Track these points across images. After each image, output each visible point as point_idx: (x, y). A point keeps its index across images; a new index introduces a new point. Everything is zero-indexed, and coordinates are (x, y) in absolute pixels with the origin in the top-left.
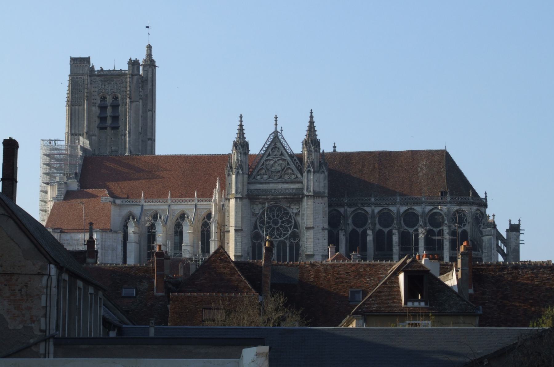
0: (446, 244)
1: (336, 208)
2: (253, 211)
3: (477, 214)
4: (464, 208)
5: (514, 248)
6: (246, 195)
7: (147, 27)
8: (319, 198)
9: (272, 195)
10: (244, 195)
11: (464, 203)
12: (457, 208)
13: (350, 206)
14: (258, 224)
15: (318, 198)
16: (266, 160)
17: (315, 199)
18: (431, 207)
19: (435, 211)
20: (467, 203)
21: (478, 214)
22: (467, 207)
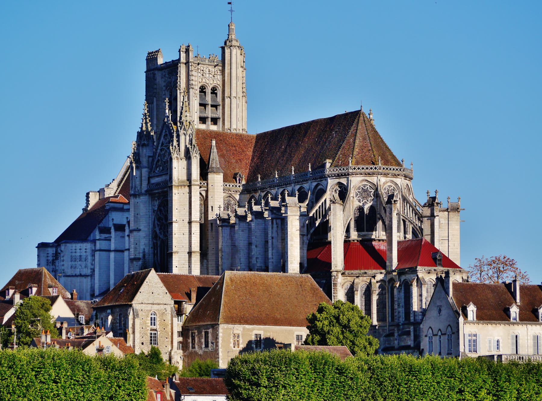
2: (154, 208)
3: (365, 185)
5: (389, 224)
6: (146, 191)
7: (230, 3)
10: (143, 191)
11: (342, 175)
13: (262, 190)
14: (156, 222)
15: (183, 187)
17: (180, 189)
18: (314, 184)
19: (320, 187)
21: (368, 186)
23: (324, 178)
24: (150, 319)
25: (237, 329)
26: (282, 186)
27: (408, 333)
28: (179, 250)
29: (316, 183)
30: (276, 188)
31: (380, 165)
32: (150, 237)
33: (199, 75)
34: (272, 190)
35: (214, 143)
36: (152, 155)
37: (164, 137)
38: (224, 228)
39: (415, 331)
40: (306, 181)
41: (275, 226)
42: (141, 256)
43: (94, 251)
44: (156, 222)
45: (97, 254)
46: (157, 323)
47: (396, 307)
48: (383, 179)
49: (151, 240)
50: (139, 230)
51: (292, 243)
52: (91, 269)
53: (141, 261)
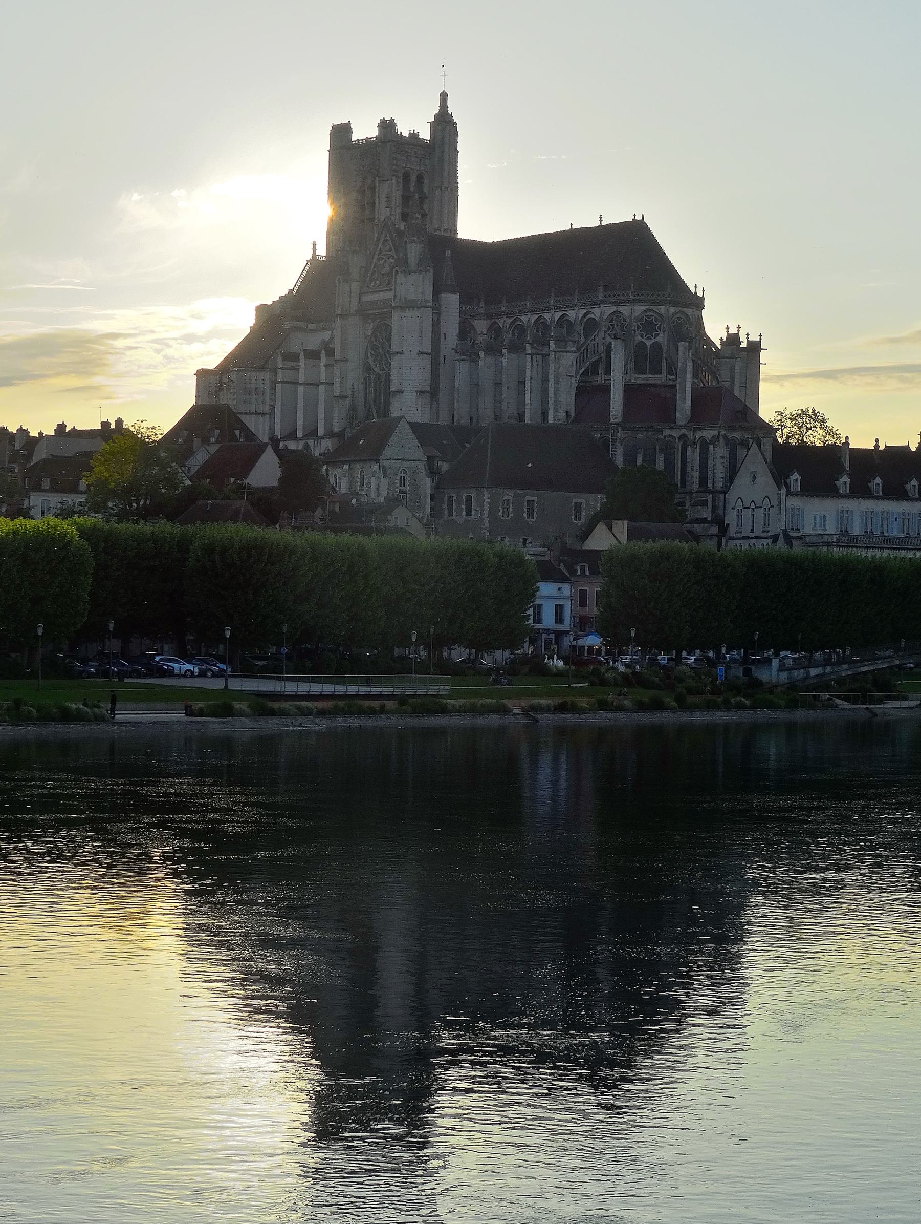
0: (552, 367)
1: (496, 320)
3: (649, 317)
4: (625, 310)
8: (413, 310)
9: (378, 309)
10: (352, 311)
11: (621, 302)
12: (615, 309)
13: (508, 315)
14: (369, 350)
15: (411, 309)
16: (379, 259)
17: (407, 312)
18: (583, 312)
19: (589, 316)
20: (625, 302)
22: (626, 307)
23: (597, 304)
24: (398, 478)
25: (508, 494)
26: (537, 311)
27: (704, 503)
28: (403, 389)
29: (585, 311)
30: (529, 314)
31: (669, 290)
32: (361, 370)
33: (404, 158)
34: (523, 317)
35: (448, 253)
36: (364, 265)
37: (383, 243)
38: (462, 362)
39: (713, 501)
40: (571, 307)
41: (535, 363)
42: (349, 393)
43: (274, 383)
44: (369, 350)
45: (279, 387)
46: (407, 483)
47: (689, 470)
48: (672, 310)
49: (361, 373)
50: (345, 360)
51: (559, 386)
52: (271, 405)
53: (348, 399)
